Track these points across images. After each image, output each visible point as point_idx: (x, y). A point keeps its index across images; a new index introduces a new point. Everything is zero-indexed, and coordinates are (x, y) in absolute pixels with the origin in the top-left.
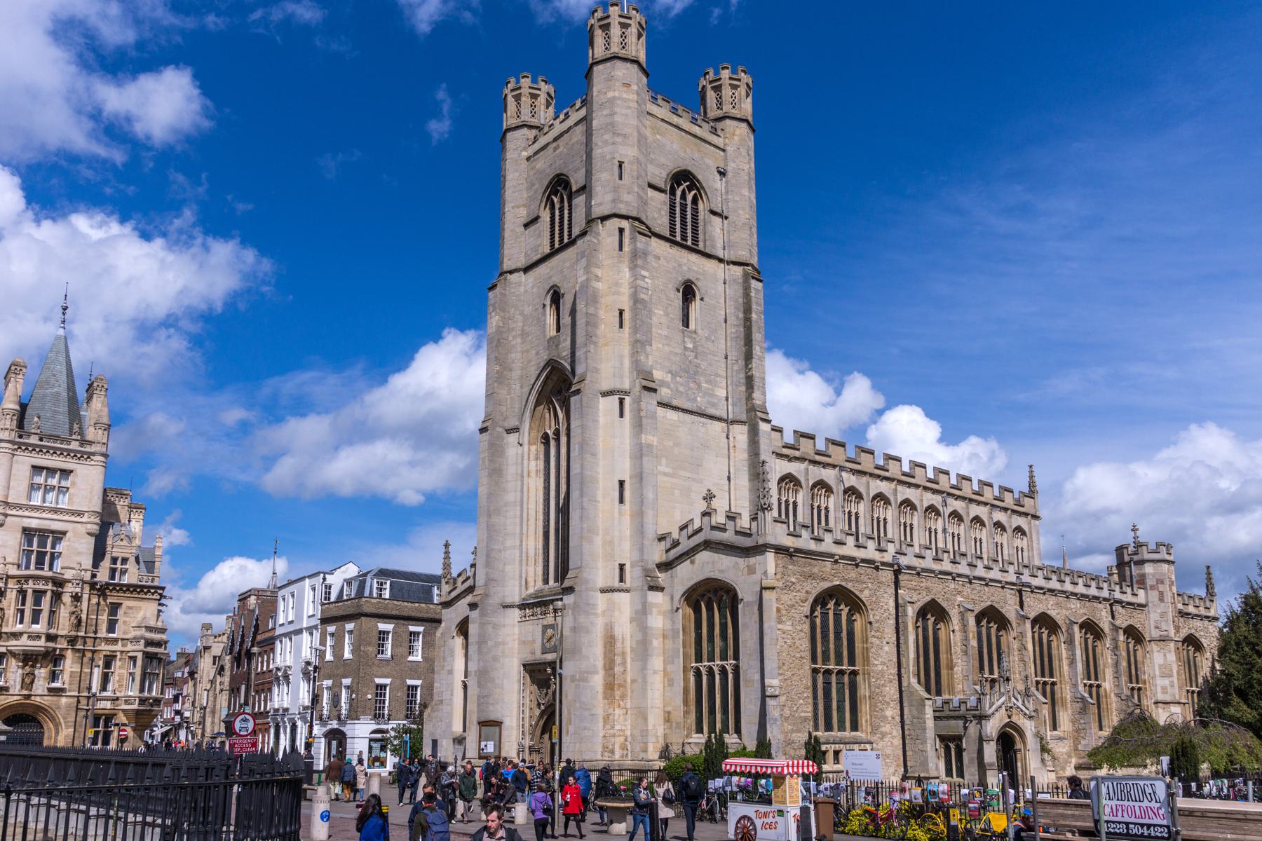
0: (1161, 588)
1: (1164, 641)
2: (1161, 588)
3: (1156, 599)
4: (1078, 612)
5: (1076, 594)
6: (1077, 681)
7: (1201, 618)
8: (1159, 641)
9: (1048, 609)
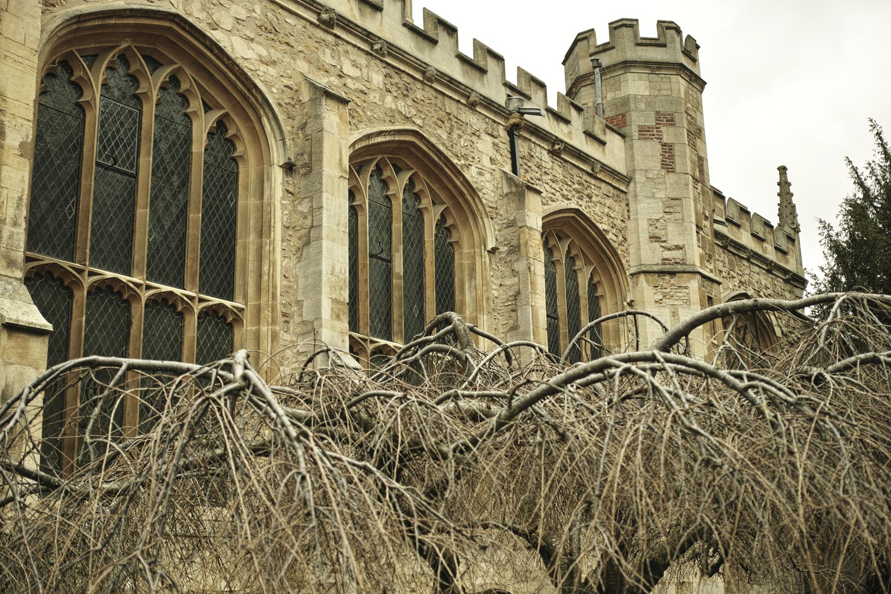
0: (668, 135)
1: (673, 274)
2: (668, 135)
3: (655, 164)
4: (374, 97)
5: (368, 36)
6: (318, 307)
7: (771, 268)
8: (661, 273)
9: (215, 26)
